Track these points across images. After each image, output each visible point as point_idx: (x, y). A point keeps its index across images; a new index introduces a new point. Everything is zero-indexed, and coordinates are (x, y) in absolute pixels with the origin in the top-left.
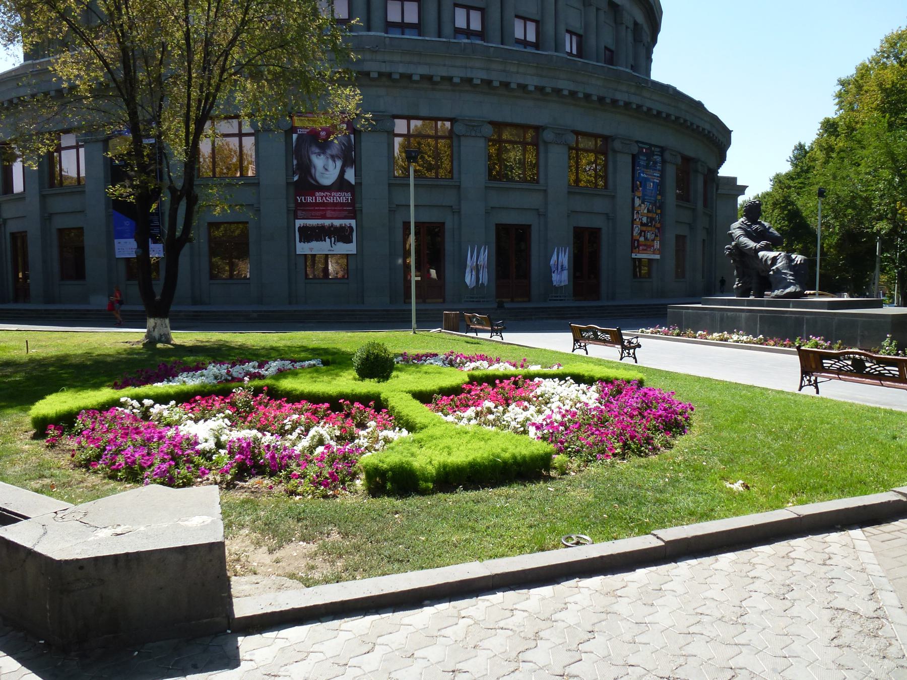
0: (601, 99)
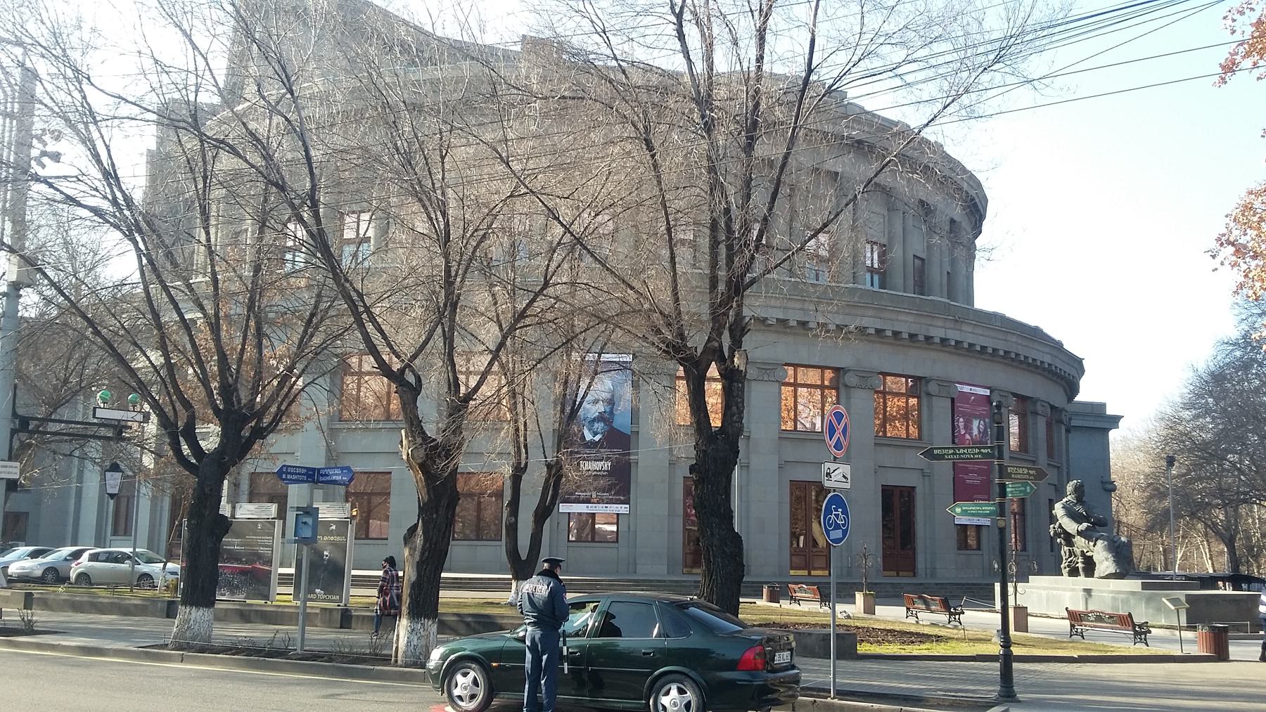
0: (912, 336)
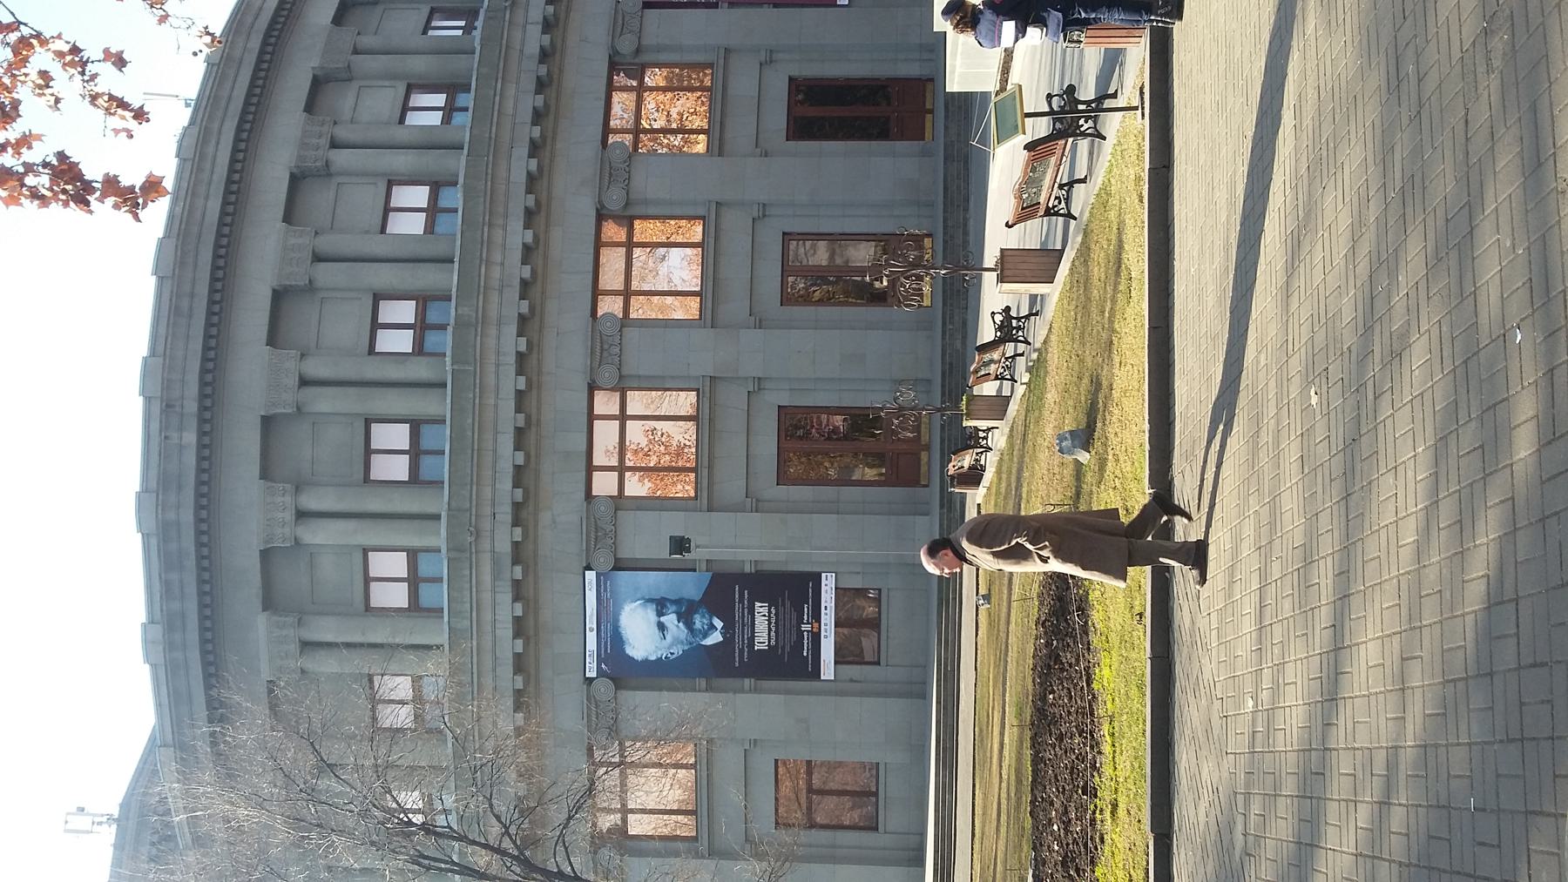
0: (541, 86)
